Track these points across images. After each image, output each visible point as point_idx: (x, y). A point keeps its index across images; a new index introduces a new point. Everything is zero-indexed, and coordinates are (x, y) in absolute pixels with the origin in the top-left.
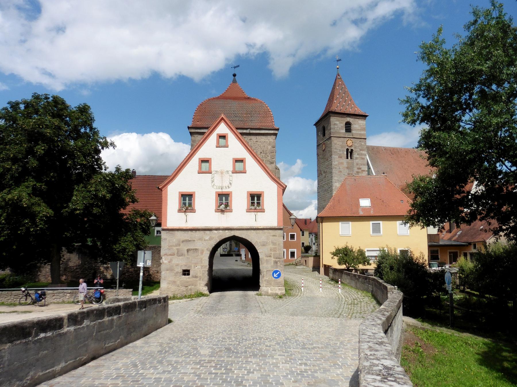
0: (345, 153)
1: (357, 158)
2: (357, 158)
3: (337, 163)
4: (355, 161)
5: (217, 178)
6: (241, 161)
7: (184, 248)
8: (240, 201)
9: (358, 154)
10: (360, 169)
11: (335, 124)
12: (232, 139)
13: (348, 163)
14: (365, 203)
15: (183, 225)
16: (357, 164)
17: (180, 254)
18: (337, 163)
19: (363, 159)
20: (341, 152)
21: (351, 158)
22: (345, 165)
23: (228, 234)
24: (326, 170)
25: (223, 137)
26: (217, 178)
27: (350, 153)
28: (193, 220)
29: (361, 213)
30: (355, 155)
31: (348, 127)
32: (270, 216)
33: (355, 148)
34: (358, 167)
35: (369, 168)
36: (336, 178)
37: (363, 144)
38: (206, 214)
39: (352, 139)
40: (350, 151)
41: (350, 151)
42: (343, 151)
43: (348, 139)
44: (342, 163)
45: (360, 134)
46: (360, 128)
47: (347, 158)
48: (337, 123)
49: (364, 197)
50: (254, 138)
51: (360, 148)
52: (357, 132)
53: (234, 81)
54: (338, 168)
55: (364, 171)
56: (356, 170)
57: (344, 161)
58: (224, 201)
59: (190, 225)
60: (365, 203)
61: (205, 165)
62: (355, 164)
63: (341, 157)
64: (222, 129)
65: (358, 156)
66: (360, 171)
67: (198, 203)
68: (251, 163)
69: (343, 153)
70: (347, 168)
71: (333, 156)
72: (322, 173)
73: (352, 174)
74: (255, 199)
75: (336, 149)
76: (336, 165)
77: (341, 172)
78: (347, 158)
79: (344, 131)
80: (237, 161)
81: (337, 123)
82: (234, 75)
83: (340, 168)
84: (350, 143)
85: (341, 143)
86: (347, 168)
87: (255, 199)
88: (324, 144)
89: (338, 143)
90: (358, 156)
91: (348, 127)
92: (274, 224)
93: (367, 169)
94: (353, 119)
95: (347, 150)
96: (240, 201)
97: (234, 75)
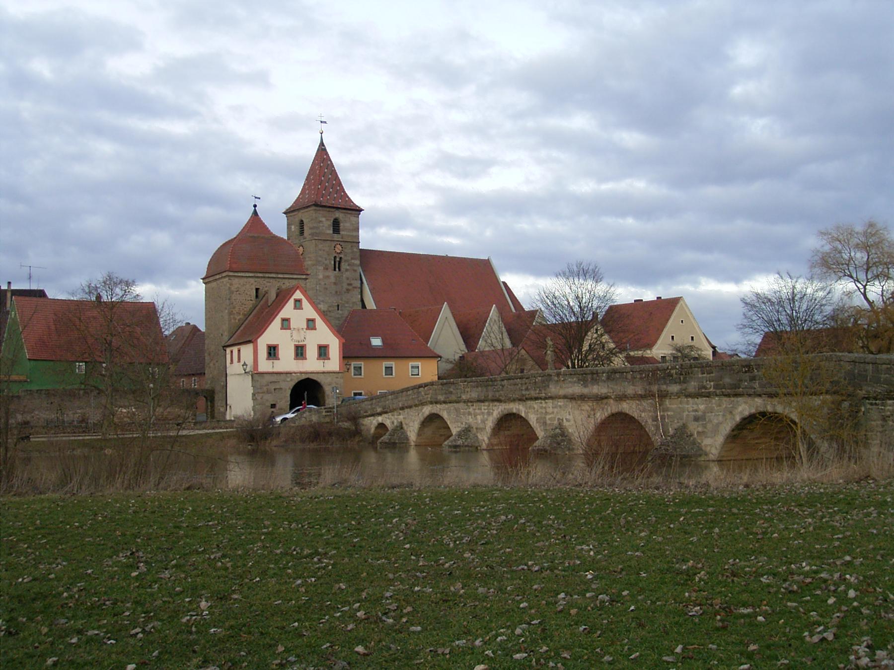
1: (347, 270)
2: (347, 270)
6: (313, 320)
7: (272, 387)
8: (312, 352)
10: (351, 284)
12: (305, 303)
13: (336, 277)
15: (271, 370)
16: (348, 279)
17: (268, 392)
19: (355, 271)
20: (327, 262)
21: (339, 270)
22: (333, 280)
23: (304, 377)
25: (298, 301)
30: (344, 266)
32: (334, 363)
34: (348, 282)
35: (362, 283)
38: (287, 363)
40: (338, 259)
41: (338, 259)
44: (328, 277)
47: (335, 270)
57: (331, 273)
58: (300, 352)
59: (275, 370)
60: (376, 342)
61: (286, 323)
64: (298, 295)
66: (350, 287)
67: (281, 352)
68: (319, 322)
70: (335, 284)
74: (323, 351)
80: (308, 320)
81: (324, 219)
82: (255, 206)
85: (327, 249)
87: (323, 351)
92: (337, 369)
95: (335, 257)
96: (312, 352)
97: (255, 206)
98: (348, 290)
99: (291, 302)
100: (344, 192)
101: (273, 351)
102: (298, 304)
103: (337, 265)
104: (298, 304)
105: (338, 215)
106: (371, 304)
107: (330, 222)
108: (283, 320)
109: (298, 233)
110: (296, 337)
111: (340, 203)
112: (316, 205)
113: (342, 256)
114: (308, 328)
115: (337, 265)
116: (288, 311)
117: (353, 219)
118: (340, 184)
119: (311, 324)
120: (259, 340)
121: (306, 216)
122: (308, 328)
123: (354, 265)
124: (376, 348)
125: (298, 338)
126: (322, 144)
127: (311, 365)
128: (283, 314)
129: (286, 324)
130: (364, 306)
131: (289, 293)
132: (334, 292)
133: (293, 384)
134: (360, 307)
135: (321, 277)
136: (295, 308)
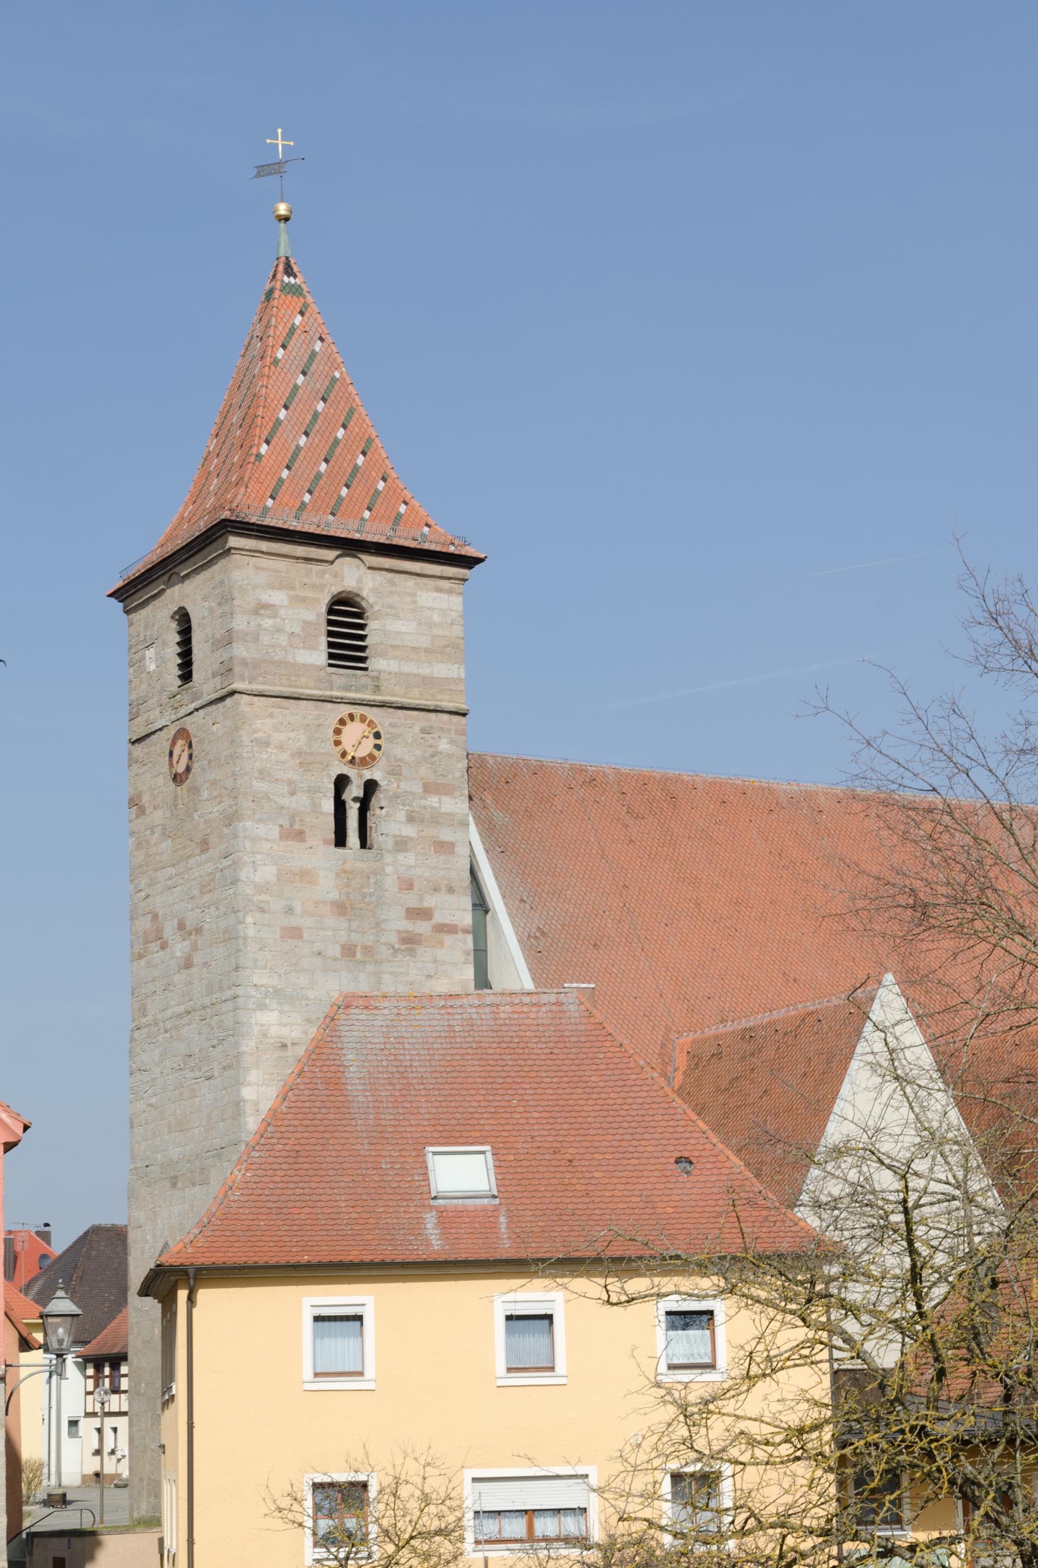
0: (328, 806)
1: (402, 844)
2: (402, 844)
3: (267, 873)
4: (394, 865)
9: (411, 819)
10: (422, 914)
11: (261, 608)
14: (461, 1173)
16: (408, 885)
18: (267, 873)
20: (300, 802)
21: (364, 842)
22: (328, 887)
24: (192, 919)
27: (353, 812)
29: (435, 1243)
30: (389, 822)
31: (346, 630)
33: (395, 772)
34: (411, 900)
36: (261, 978)
37: (444, 746)
39: (371, 713)
40: (355, 790)
41: (355, 790)
42: (314, 791)
43: (345, 710)
44: (306, 876)
45: (427, 682)
46: (425, 642)
47: (340, 840)
48: (278, 597)
49: (457, 1135)
51: (424, 771)
52: (409, 668)
54: (277, 905)
55: (450, 929)
56: (397, 922)
57: (319, 854)
60: (461, 1173)
62: (390, 883)
63: (300, 836)
65: (410, 831)
66: (422, 927)
69: (316, 808)
70: (341, 908)
71: (248, 826)
72: (169, 930)
73: (368, 950)
75: (263, 774)
76: (260, 889)
77: (294, 933)
78: (340, 840)
79: (320, 656)
81: (278, 597)
83: (290, 910)
84: (356, 738)
85: (299, 740)
86: (341, 908)
88: (183, 733)
89: (278, 737)
90: (410, 831)
91: (346, 630)
93: (467, 919)
94: (380, 577)
95: (341, 783)
98: (410, 941)
105: (351, 574)
107: (317, 613)
113: (375, 774)
132: (335, 951)
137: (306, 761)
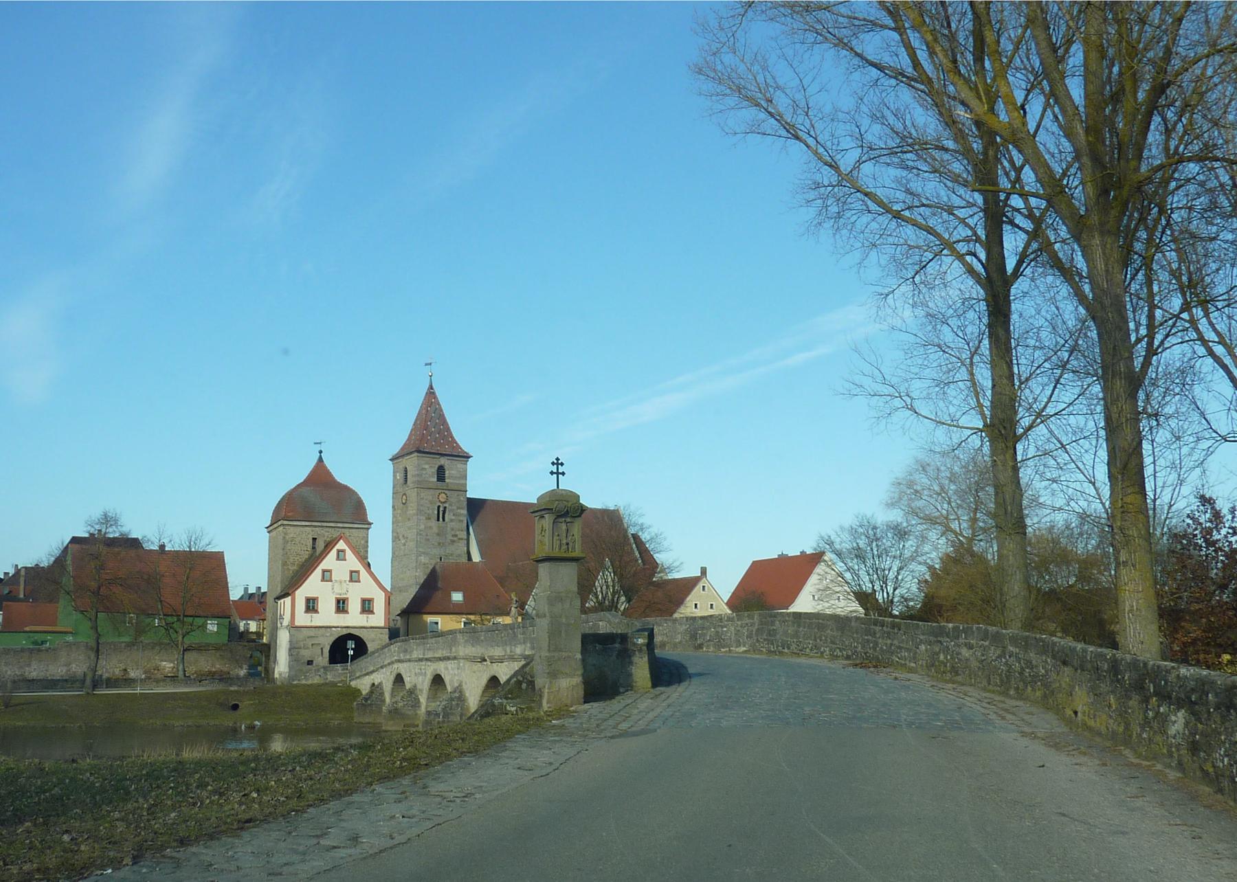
1: (452, 520)
2: (452, 520)
5: (336, 585)
6: (358, 572)
8: (354, 606)
12: (349, 554)
14: (457, 597)
15: (309, 624)
22: (435, 530)
23: (345, 632)
26: (336, 585)
28: (317, 620)
35: (468, 533)
38: (327, 616)
49: (456, 590)
50: (346, 531)
53: (321, 460)
57: (433, 523)
58: (341, 606)
59: (313, 624)
60: (457, 597)
64: (341, 545)
67: (321, 606)
80: (352, 572)
82: (321, 452)
96: (354, 606)
97: (321, 452)
98: (453, 542)
99: (333, 553)
100: (452, 437)
101: (311, 605)
102: (341, 556)
103: (441, 515)
104: (341, 556)
106: (476, 557)
107: (435, 470)
108: (324, 571)
109: (402, 481)
110: (337, 590)
111: (447, 449)
112: (419, 452)
114: (351, 580)
115: (441, 515)
116: (330, 561)
117: (460, 466)
118: (448, 429)
119: (354, 576)
120: (297, 592)
121: (411, 462)
122: (351, 580)
123: (460, 515)
124: (457, 604)
125: (340, 591)
126: (431, 387)
127: (354, 619)
128: (324, 565)
129: (326, 576)
130: (470, 558)
131: (329, 546)
133: (333, 639)
134: (464, 559)
135: (422, 527)
136: (338, 558)
137: (431, 502)
